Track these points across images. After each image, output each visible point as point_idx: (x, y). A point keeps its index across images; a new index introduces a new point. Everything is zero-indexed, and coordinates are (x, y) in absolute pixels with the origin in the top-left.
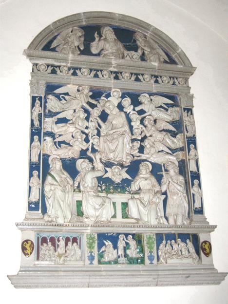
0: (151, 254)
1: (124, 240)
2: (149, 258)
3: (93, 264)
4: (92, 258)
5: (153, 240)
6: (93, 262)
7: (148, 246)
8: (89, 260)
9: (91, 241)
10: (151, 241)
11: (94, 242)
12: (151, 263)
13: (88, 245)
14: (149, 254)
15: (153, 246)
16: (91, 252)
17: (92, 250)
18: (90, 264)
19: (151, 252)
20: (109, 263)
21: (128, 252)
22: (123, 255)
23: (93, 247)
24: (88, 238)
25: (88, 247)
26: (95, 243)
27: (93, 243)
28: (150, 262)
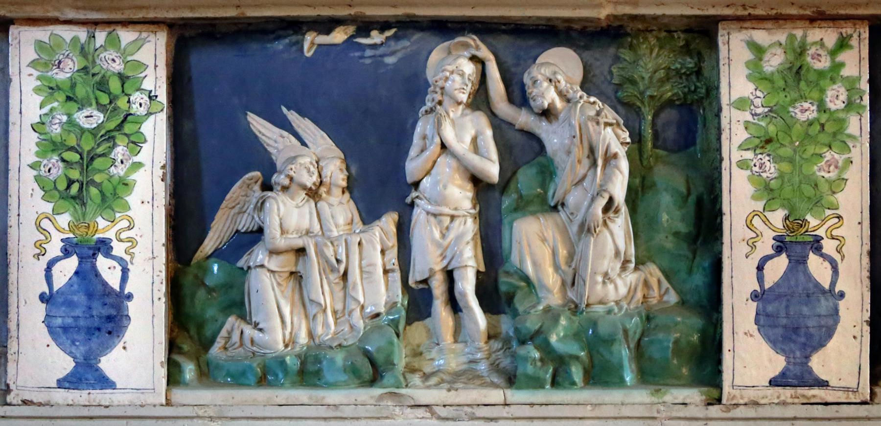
0: (798, 263)
1: (480, 99)
2: (765, 321)
3: (105, 383)
4: (91, 316)
5: (836, 97)
6: (111, 363)
7: (771, 170)
8: (60, 333)
9: (90, 118)
10: (805, 112)
11: (122, 127)
12: (797, 377)
13: (59, 172)
14: (779, 266)
15: (822, 172)
16: (87, 249)
17: (104, 228)
18: (69, 382)
19: (795, 245)
20: (308, 371)
21: (534, 243)
22: (467, 285)
23: (113, 197)
24: (53, 89)
25: (49, 190)
26: (136, 143)
27: (110, 138)
28: (777, 364)
